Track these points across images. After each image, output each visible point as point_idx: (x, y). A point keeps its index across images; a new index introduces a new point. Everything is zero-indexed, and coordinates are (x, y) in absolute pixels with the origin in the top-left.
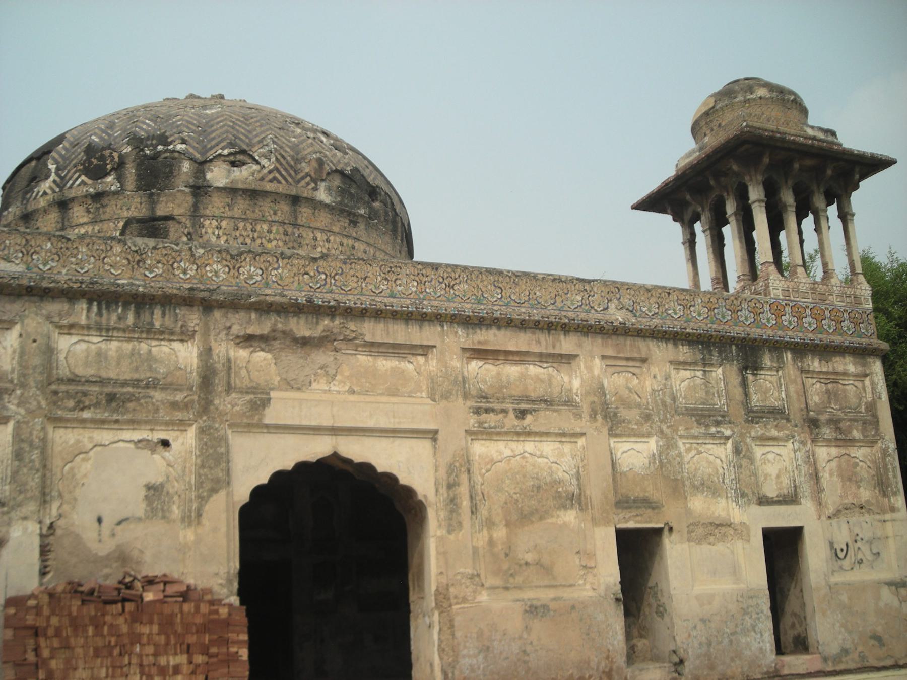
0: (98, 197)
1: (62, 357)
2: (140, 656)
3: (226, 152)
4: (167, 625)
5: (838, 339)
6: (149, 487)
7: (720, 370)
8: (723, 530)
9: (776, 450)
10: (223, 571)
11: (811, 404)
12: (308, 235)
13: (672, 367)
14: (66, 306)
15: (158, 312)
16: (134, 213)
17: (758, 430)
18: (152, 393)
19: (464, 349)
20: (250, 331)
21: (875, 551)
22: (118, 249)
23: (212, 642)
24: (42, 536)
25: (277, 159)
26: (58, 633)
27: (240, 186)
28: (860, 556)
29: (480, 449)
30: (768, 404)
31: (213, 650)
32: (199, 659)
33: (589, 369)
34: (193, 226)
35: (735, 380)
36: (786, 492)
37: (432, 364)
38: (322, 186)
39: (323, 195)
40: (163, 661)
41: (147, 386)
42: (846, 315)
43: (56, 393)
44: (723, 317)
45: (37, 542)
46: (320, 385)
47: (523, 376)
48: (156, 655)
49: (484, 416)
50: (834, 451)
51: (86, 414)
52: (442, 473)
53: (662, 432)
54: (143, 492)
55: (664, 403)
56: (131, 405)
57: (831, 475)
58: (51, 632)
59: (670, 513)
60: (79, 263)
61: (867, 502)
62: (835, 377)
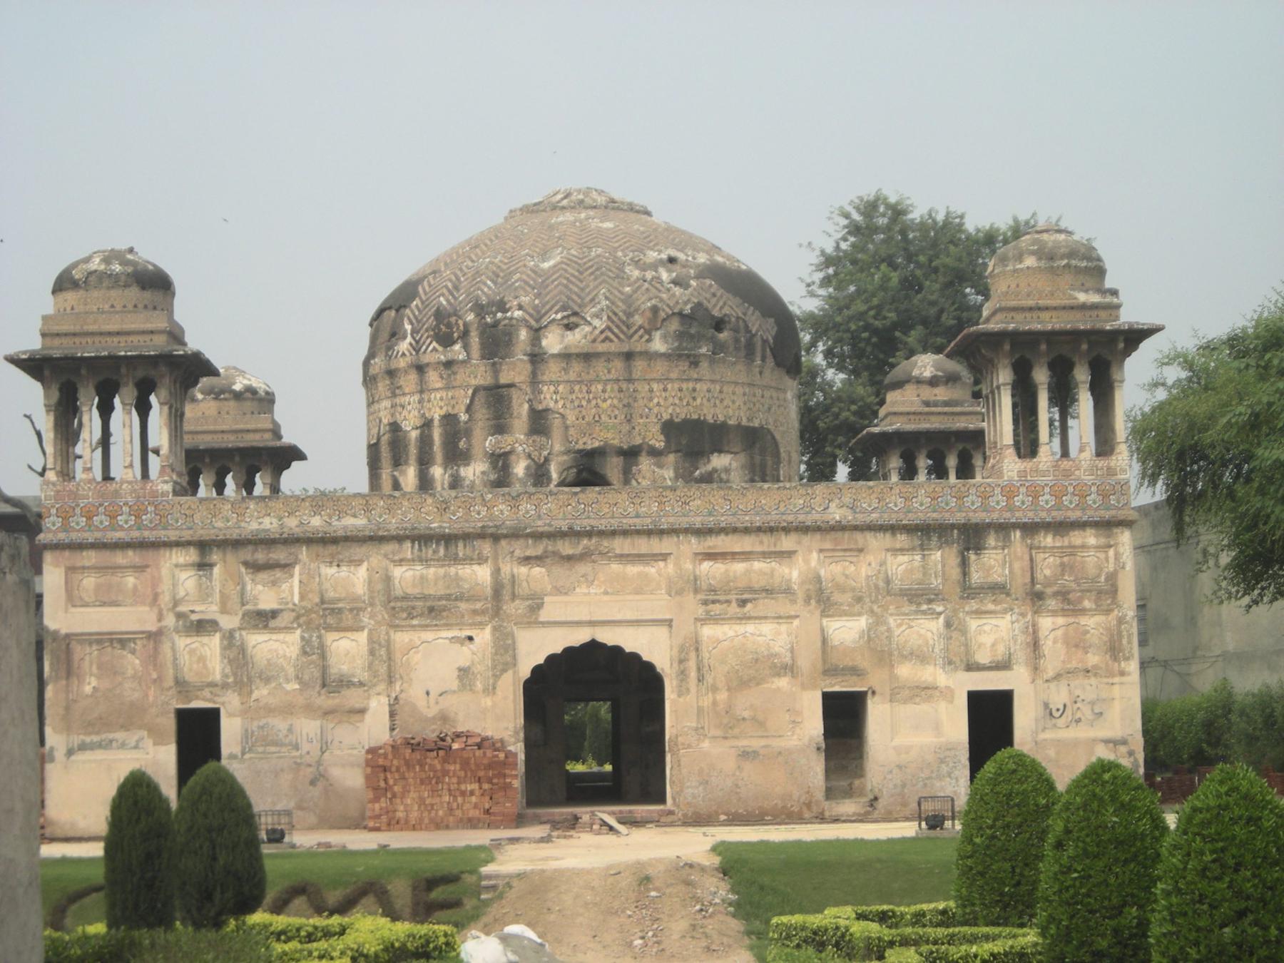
0: (449, 364)
1: (397, 582)
2: (449, 784)
3: (559, 316)
4: (465, 764)
5: (1074, 515)
6: (460, 669)
7: (939, 553)
8: (929, 692)
9: (994, 621)
10: (511, 726)
11: (1039, 577)
12: (643, 388)
13: (889, 554)
14: (397, 546)
15: (461, 544)
16: (482, 382)
17: (973, 605)
18: (459, 604)
19: (696, 554)
20: (528, 553)
21: (1097, 711)
22: (430, 501)
23: (495, 776)
24: (390, 705)
25: (609, 317)
26: (398, 770)
27: (573, 351)
28: (1078, 715)
29: (707, 631)
30: (990, 580)
31: (495, 781)
32: (486, 786)
33: (807, 561)
34: (533, 393)
35: (953, 560)
36: (1000, 658)
37: (669, 568)
38: (657, 335)
39: (658, 345)
40: (463, 787)
41: (456, 599)
42: (1094, 489)
43: (394, 608)
44: (947, 504)
45: (387, 709)
46: (582, 590)
47: (748, 571)
48: (458, 783)
49: (711, 607)
50: (1061, 621)
51: (415, 622)
52: (675, 650)
53: (872, 611)
54: (456, 673)
55: (876, 587)
56: (444, 614)
57: (1055, 642)
58: (394, 769)
59: (874, 679)
60: (404, 514)
61: (1095, 667)
62: (1073, 550)
